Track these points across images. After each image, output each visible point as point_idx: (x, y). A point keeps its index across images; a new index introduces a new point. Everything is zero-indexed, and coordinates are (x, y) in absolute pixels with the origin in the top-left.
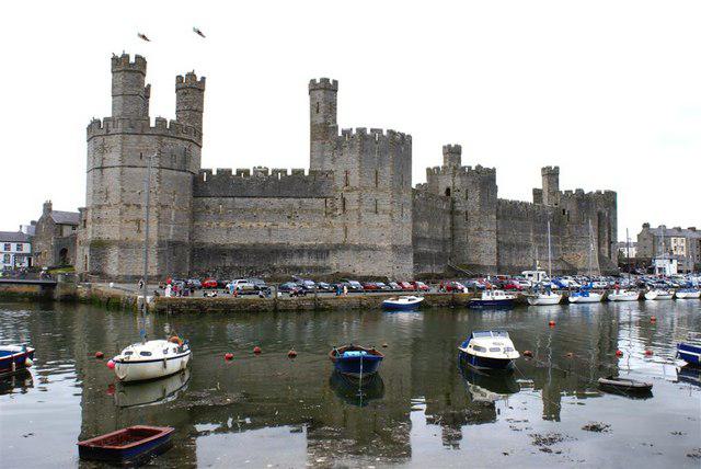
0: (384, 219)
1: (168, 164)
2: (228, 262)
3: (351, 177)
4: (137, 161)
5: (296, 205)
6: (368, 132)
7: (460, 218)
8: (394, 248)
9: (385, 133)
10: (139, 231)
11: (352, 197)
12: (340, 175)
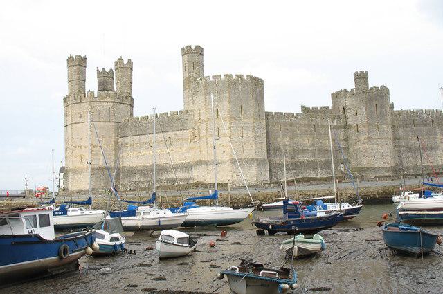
0: (224, 140)
1: (97, 119)
2: (138, 178)
3: (202, 113)
4: (78, 120)
5: (173, 137)
6: (211, 79)
7: (352, 131)
8: (233, 161)
9: (223, 77)
10: (82, 162)
11: (203, 127)
12: (196, 112)
